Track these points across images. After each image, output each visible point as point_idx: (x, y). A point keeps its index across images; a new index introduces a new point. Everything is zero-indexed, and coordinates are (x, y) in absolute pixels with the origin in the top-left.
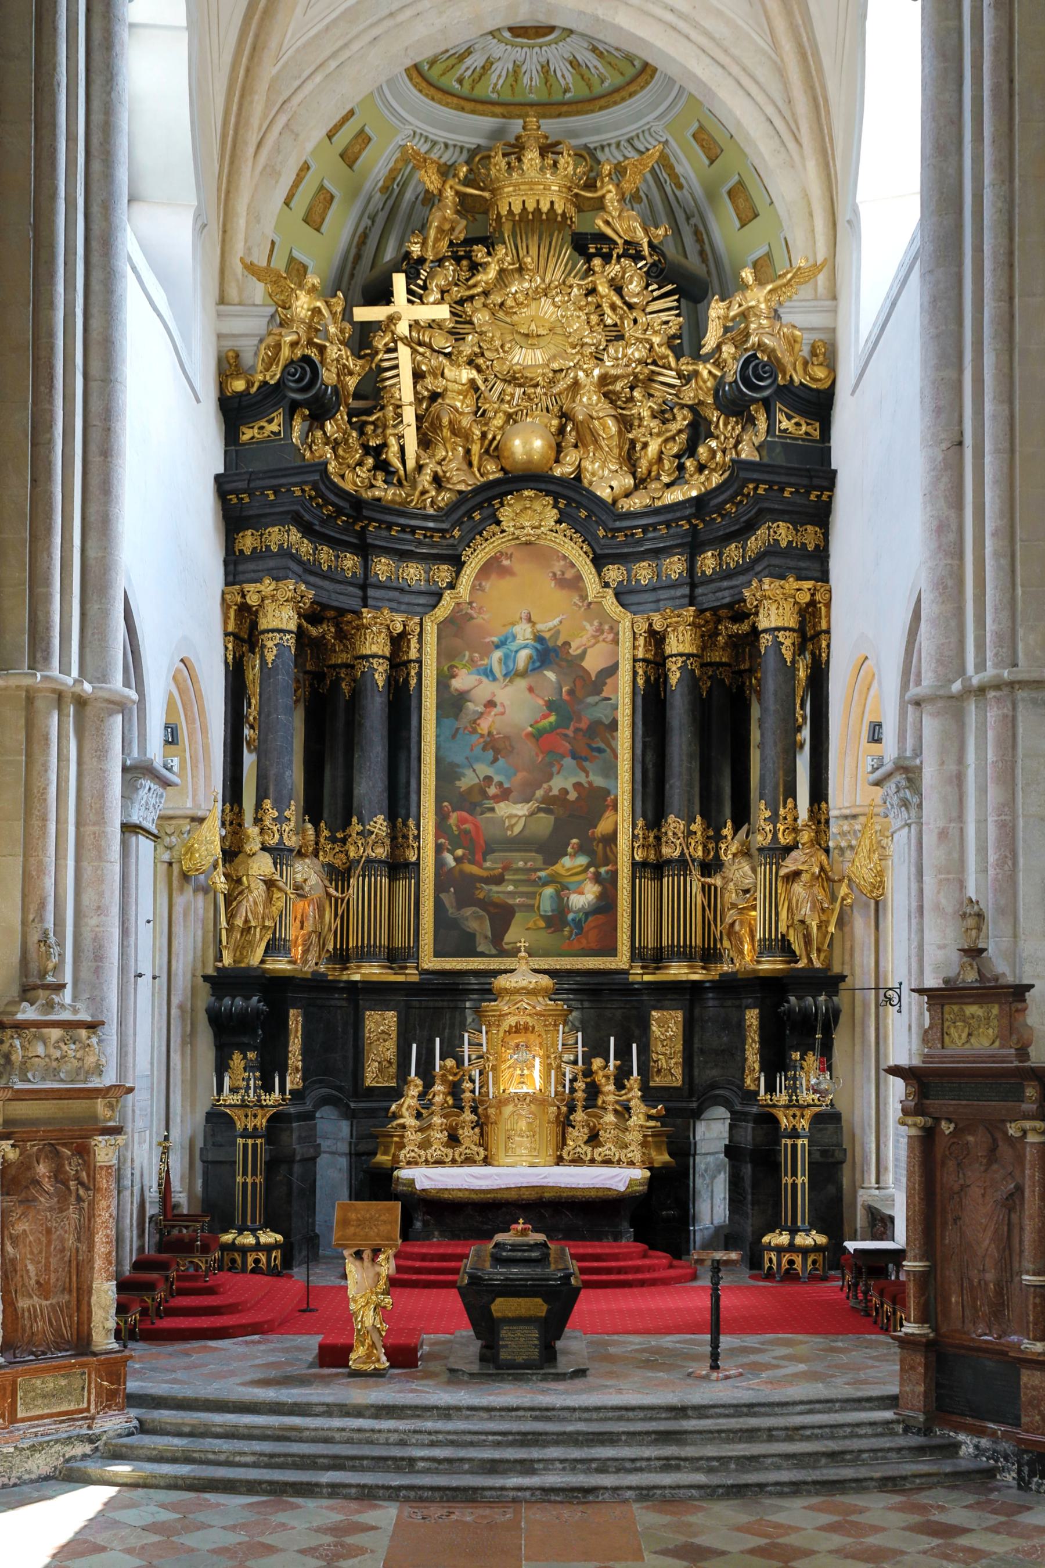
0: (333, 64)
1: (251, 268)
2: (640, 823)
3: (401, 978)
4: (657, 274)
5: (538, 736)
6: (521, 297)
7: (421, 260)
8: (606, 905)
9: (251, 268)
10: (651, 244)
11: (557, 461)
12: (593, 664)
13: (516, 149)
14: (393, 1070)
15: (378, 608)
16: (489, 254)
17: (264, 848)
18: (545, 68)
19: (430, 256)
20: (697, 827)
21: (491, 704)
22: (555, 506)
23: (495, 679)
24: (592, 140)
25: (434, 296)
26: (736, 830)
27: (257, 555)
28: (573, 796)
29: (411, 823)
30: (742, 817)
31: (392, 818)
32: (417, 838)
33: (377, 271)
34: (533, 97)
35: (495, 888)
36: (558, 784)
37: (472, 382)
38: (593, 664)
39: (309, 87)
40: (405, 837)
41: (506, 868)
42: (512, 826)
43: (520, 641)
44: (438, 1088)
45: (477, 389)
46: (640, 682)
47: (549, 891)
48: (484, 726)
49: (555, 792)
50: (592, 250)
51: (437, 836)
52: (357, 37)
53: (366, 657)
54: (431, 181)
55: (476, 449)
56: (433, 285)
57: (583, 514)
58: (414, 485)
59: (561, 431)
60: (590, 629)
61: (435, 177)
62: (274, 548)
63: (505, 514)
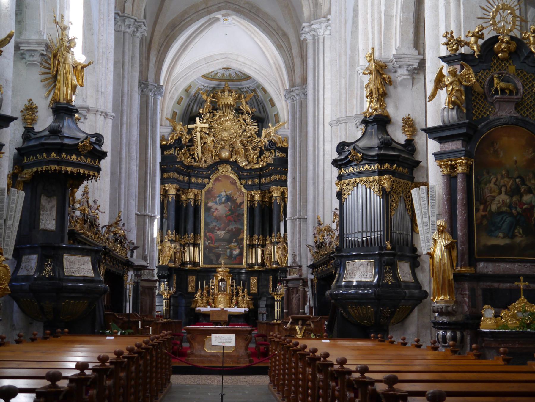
0: (185, 77)
1: (167, 119)
2: (248, 236)
3: (196, 269)
4: (254, 118)
5: (226, 216)
6: (224, 121)
7: (202, 114)
8: (241, 254)
9: (167, 119)
10: (252, 112)
11: (231, 157)
12: (239, 201)
13: (223, 92)
14: (194, 289)
15: (192, 189)
16: (217, 112)
17: (169, 240)
18: (230, 74)
19: (204, 113)
20: (261, 237)
21: (216, 209)
22: (231, 167)
23: (217, 204)
24: (239, 87)
25: (205, 121)
26: (269, 238)
27: (168, 178)
28: (234, 230)
29: (199, 235)
30: (271, 235)
31: (194, 234)
32: (200, 238)
33: (192, 115)
34: (227, 78)
35: (217, 250)
36: (231, 227)
37: (213, 141)
38: (239, 201)
39: (180, 81)
40: (197, 238)
41: (220, 245)
42: (221, 236)
43: (223, 196)
44: (205, 291)
45: (214, 141)
46: (249, 205)
47: (229, 250)
48: (215, 214)
49: (230, 229)
50: (239, 112)
51: (204, 238)
52: (190, 71)
53: (189, 199)
54: (205, 97)
55: (213, 154)
56: (205, 118)
57: (237, 169)
58: (200, 162)
59: (232, 151)
60: (238, 194)
61: (205, 96)
62: (171, 177)
63: (220, 169)
